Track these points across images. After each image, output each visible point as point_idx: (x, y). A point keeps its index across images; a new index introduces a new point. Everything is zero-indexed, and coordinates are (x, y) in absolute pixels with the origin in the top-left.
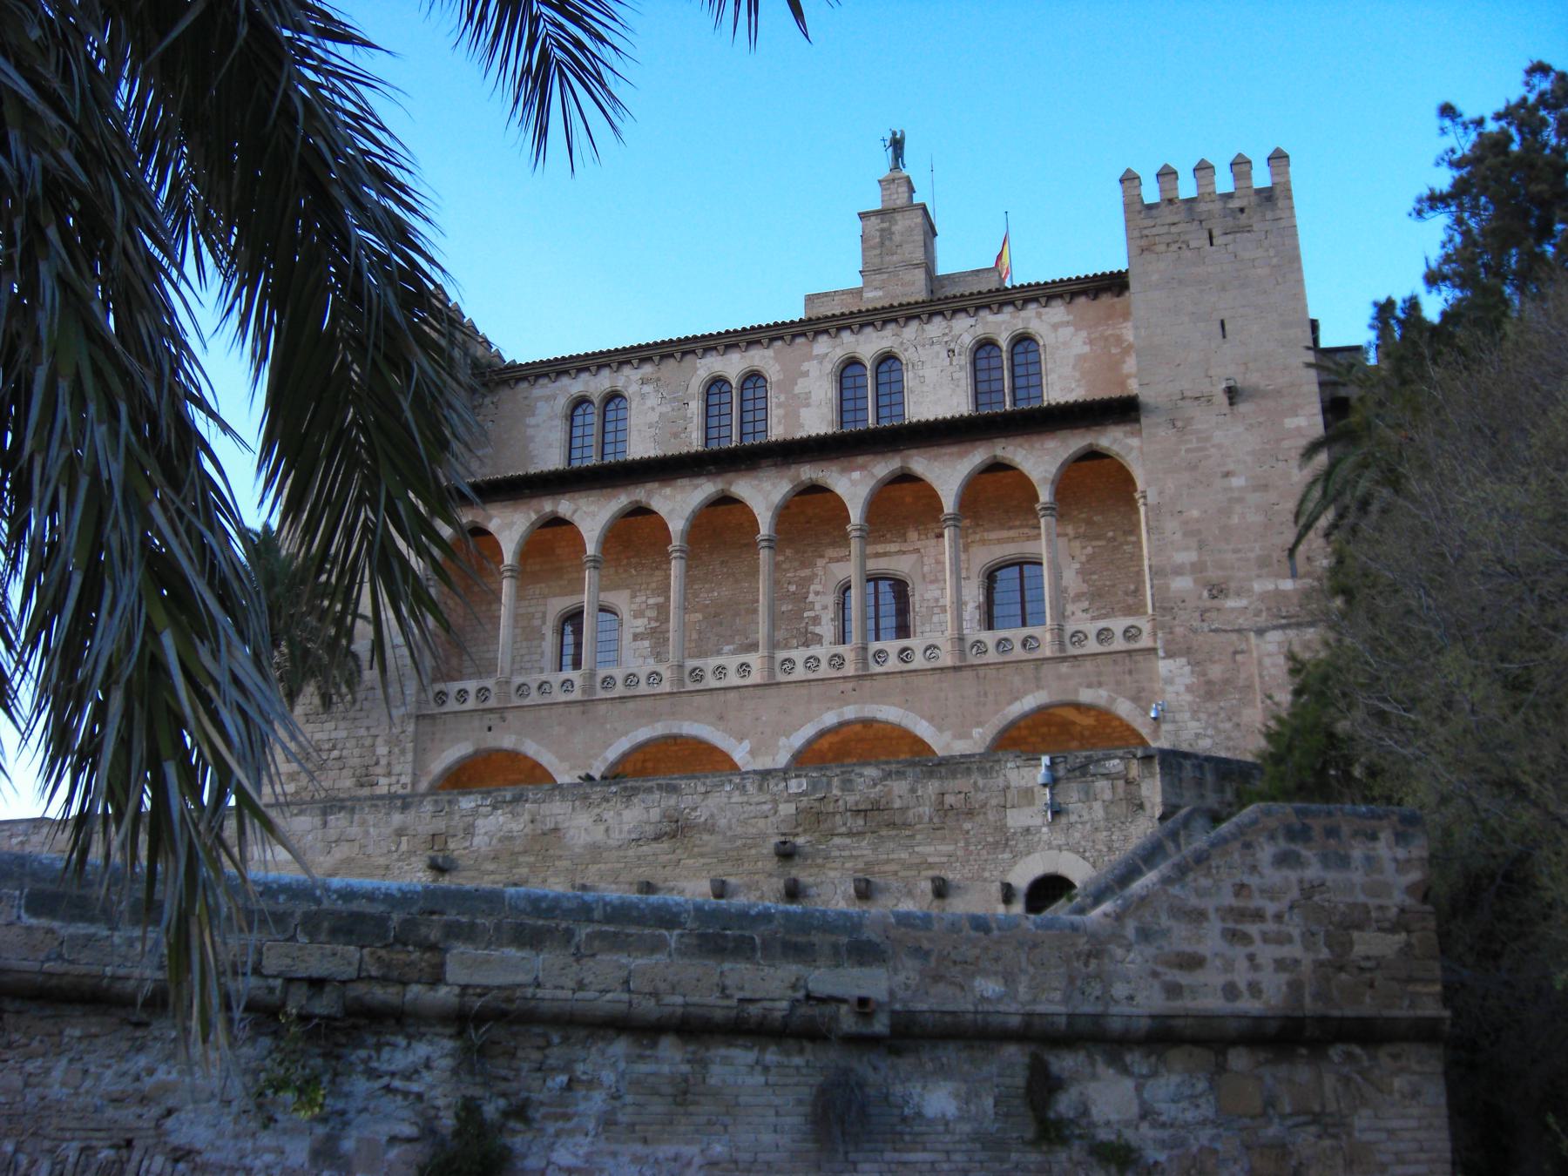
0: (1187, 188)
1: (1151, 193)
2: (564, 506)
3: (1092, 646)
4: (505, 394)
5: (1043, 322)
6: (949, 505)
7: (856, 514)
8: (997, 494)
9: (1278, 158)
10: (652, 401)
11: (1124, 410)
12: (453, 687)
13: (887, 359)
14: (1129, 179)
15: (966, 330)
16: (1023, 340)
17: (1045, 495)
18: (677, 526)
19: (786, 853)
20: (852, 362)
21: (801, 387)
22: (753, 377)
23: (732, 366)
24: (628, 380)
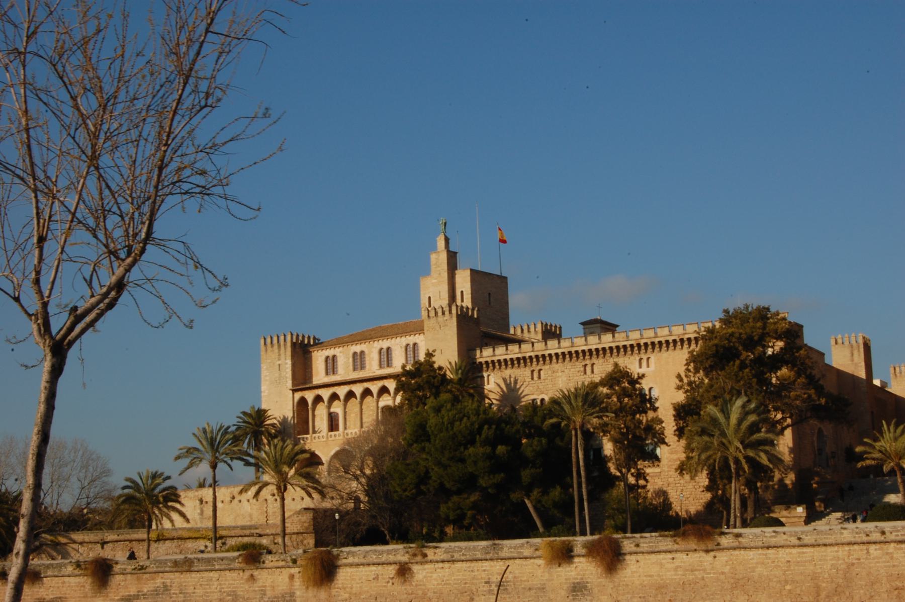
13: (388, 349)
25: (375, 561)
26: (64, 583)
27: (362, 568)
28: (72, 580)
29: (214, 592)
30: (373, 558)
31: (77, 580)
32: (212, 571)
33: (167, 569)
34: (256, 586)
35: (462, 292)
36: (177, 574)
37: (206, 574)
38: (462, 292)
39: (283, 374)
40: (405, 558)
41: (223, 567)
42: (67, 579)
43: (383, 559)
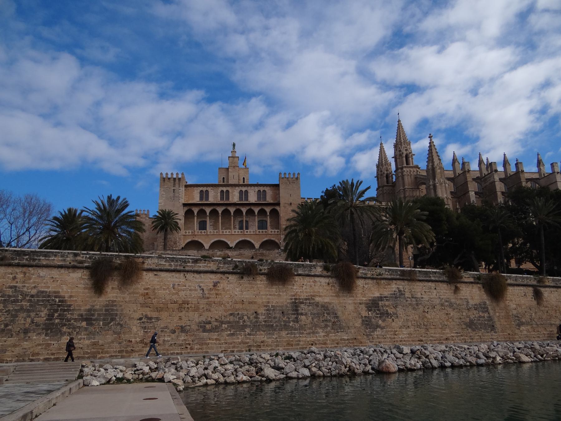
0: (287, 176)
2: (204, 208)
3: (273, 233)
4: (189, 188)
5: (267, 189)
6: (256, 214)
7: (244, 214)
8: (262, 212)
10: (213, 192)
12: (187, 231)
13: (246, 191)
14: (280, 174)
15: (257, 189)
16: (264, 191)
17: (268, 214)
18: (220, 212)
20: (241, 191)
21: (234, 193)
22: (228, 191)
23: (225, 189)
24: (209, 189)
25: (522, 283)
27: (516, 288)
28: (324, 281)
29: (436, 298)
30: (520, 282)
31: (327, 280)
32: (428, 281)
33: (398, 277)
35: (244, 178)
36: (406, 282)
38: (244, 178)
39: (177, 195)
40: (535, 283)
42: (317, 279)
43: (525, 283)
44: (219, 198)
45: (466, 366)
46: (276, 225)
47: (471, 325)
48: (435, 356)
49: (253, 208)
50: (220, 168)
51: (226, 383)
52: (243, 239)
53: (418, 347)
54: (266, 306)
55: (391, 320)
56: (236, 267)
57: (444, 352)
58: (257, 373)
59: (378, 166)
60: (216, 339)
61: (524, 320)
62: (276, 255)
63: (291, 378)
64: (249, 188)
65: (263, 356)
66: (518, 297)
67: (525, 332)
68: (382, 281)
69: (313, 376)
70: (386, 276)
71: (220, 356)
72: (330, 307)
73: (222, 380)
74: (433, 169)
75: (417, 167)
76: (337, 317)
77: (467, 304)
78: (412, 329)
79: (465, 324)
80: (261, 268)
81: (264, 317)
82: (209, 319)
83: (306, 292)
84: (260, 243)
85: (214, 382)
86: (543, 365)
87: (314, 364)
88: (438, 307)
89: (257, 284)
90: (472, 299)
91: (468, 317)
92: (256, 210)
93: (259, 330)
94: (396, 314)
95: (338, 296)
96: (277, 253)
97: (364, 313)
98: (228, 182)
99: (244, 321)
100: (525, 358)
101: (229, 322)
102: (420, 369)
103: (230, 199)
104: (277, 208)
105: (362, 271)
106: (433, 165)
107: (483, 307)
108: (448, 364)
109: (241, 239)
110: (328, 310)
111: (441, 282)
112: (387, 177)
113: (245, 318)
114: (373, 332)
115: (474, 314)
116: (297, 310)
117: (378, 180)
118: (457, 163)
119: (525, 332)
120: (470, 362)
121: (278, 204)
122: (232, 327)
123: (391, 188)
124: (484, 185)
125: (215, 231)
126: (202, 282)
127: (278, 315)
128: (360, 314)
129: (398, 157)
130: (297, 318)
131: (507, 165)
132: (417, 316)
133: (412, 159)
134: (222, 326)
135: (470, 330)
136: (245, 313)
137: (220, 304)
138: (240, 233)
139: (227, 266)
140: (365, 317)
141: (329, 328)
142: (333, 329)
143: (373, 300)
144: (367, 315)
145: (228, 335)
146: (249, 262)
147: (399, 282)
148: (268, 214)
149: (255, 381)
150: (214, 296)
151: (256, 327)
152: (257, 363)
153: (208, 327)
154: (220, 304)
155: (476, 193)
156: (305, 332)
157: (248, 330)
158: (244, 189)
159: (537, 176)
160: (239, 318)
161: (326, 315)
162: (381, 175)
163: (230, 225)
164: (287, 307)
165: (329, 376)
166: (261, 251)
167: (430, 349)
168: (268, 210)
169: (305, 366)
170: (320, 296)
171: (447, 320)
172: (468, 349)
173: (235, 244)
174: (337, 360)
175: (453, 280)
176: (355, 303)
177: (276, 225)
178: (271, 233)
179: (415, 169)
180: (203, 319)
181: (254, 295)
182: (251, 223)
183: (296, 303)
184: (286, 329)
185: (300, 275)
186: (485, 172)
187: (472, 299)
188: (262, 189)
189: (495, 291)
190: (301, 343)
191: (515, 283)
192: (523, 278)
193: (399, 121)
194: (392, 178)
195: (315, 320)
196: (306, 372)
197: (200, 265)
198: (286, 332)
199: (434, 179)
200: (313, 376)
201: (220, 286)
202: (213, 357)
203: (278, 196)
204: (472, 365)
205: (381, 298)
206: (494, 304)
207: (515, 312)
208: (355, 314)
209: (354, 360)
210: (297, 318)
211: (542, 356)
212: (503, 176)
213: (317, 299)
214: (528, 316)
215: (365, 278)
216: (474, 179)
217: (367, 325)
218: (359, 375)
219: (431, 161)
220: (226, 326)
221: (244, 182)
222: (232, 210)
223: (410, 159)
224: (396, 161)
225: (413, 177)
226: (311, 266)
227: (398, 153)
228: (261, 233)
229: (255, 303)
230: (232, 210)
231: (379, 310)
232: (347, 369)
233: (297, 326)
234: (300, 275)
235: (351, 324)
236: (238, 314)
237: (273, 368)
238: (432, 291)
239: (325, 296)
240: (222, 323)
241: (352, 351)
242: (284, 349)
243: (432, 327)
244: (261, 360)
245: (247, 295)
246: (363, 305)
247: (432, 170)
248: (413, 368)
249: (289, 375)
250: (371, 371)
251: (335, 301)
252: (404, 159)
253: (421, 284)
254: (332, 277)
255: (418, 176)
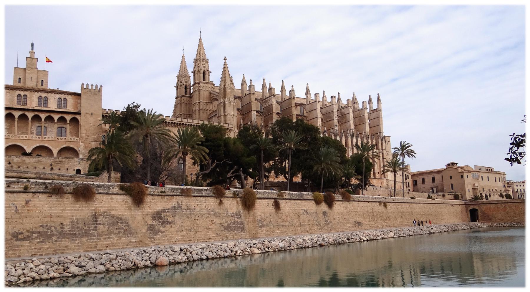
0: (90, 87)
1: (85, 87)
3: (72, 140)
5: (69, 97)
6: (56, 121)
7: (43, 120)
8: (62, 120)
9: (101, 86)
11: (79, 114)
14: (83, 84)
15: (58, 96)
17: (68, 122)
18: (16, 117)
19: (51, 165)
21: (33, 98)
22: (25, 96)
23: (22, 93)
26: (112, 199)
27: (263, 200)
28: (120, 198)
29: (204, 209)
30: (266, 196)
33: (178, 194)
34: (223, 207)
35: (42, 81)
37: (199, 198)
38: (42, 81)
40: (276, 196)
41: (207, 195)
42: (114, 196)
43: (269, 197)
44: (16, 102)
45: (216, 258)
46: (77, 133)
47: (228, 228)
48: (196, 252)
49: (52, 115)
50: (15, 68)
51: (41, 280)
52: (41, 144)
53: (186, 246)
54: (71, 219)
55: (169, 226)
56: (46, 187)
57: (203, 249)
58: (64, 271)
59: (178, 77)
60: (27, 246)
61: (265, 223)
62: (75, 163)
63: (91, 273)
64: (49, 94)
65: (69, 257)
66: (263, 206)
67: (265, 232)
68: (166, 197)
69: (107, 271)
70: (169, 194)
71: (33, 260)
72: (123, 218)
73: (37, 278)
74: (225, 89)
75: (212, 83)
76: (128, 226)
77: (227, 213)
78: (184, 233)
79: (224, 227)
80: (68, 188)
81: (69, 227)
82: (22, 230)
83: (105, 207)
84: (58, 149)
85: (31, 279)
86: (269, 255)
87: (108, 262)
88: (206, 216)
89: (64, 201)
90: (231, 209)
91: (227, 222)
92: (56, 117)
93: (64, 237)
94: (174, 221)
95: (130, 209)
96: (77, 162)
97: (150, 222)
98: (25, 83)
99: (52, 231)
100: (256, 251)
101: (39, 232)
102: (185, 262)
103: (28, 104)
104: (77, 117)
105: (151, 189)
106: (225, 86)
107: (238, 215)
108: (205, 257)
109: (38, 145)
110: (122, 220)
111: (210, 197)
112: (186, 88)
113: (53, 228)
114: (155, 235)
115: (230, 220)
116: (96, 221)
117: (177, 90)
118: (245, 85)
119: (265, 232)
120: (220, 255)
121: (79, 114)
122: (41, 236)
123: (188, 98)
124: (264, 106)
125: (11, 135)
126: (14, 201)
127: (80, 226)
128: (146, 222)
129: (196, 72)
130: (96, 227)
131: (284, 90)
132: (189, 223)
133: (209, 76)
134: (32, 236)
135: (226, 232)
136: (53, 224)
137: (31, 218)
138: (37, 139)
139: (38, 187)
140: (150, 224)
141: (121, 234)
142: (124, 234)
143: (157, 212)
144: (152, 223)
145: (38, 242)
146: (57, 183)
147: (178, 198)
148: (68, 122)
149: (63, 277)
150: (26, 211)
151: (62, 235)
152: (64, 264)
153: (20, 236)
154: (31, 218)
155: (257, 112)
156: (102, 238)
157: (54, 238)
158: (43, 95)
159: (304, 102)
160: (48, 229)
161: (119, 224)
162: (181, 86)
163: (27, 130)
164: (88, 219)
165: (118, 271)
166: (60, 159)
167: (194, 247)
168: (68, 118)
169: (102, 264)
170: (116, 210)
171: (211, 225)
172: (221, 246)
173: (32, 149)
174: (125, 258)
175: (219, 195)
176: (143, 215)
177: (77, 133)
178: (70, 140)
179: (210, 86)
180: (16, 230)
181: (61, 210)
182: (50, 129)
183: (96, 215)
184: (87, 236)
185: (100, 193)
186: (268, 95)
187: (231, 209)
188: (63, 97)
189: (248, 203)
190: (99, 246)
191: (263, 197)
192: (269, 193)
193: (200, 39)
194: (190, 90)
195: (111, 228)
196: (102, 268)
197: (14, 186)
198: (87, 238)
199: (225, 97)
200: (107, 271)
201: (32, 203)
202: (28, 261)
203: (79, 105)
204: (220, 258)
205: (164, 210)
206: (247, 212)
207: (259, 218)
208: (143, 223)
209: (138, 258)
210: (96, 227)
211: (268, 248)
212: (280, 100)
213: (113, 212)
214: (268, 220)
215: (153, 195)
216: (257, 100)
217: (151, 230)
218: (141, 268)
219: (223, 82)
220: (36, 235)
221: (42, 85)
222: (30, 115)
223: (207, 76)
224: (194, 76)
225: (208, 92)
226: (109, 187)
227: (197, 69)
228: (60, 140)
229: (62, 216)
230: (30, 115)
231: (161, 219)
232: (133, 264)
233: (96, 233)
234: (100, 193)
235: (139, 230)
236: (47, 226)
237: (77, 266)
238: (203, 203)
239: (120, 210)
240: (33, 233)
241: (137, 251)
242: (84, 251)
243: (200, 230)
244: (68, 261)
245: (55, 211)
246: (149, 216)
247: (224, 90)
248: (179, 261)
249: (89, 271)
250: (150, 265)
251: (128, 213)
252: (202, 75)
253: (195, 199)
254: (126, 195)
255: (212, 92)
